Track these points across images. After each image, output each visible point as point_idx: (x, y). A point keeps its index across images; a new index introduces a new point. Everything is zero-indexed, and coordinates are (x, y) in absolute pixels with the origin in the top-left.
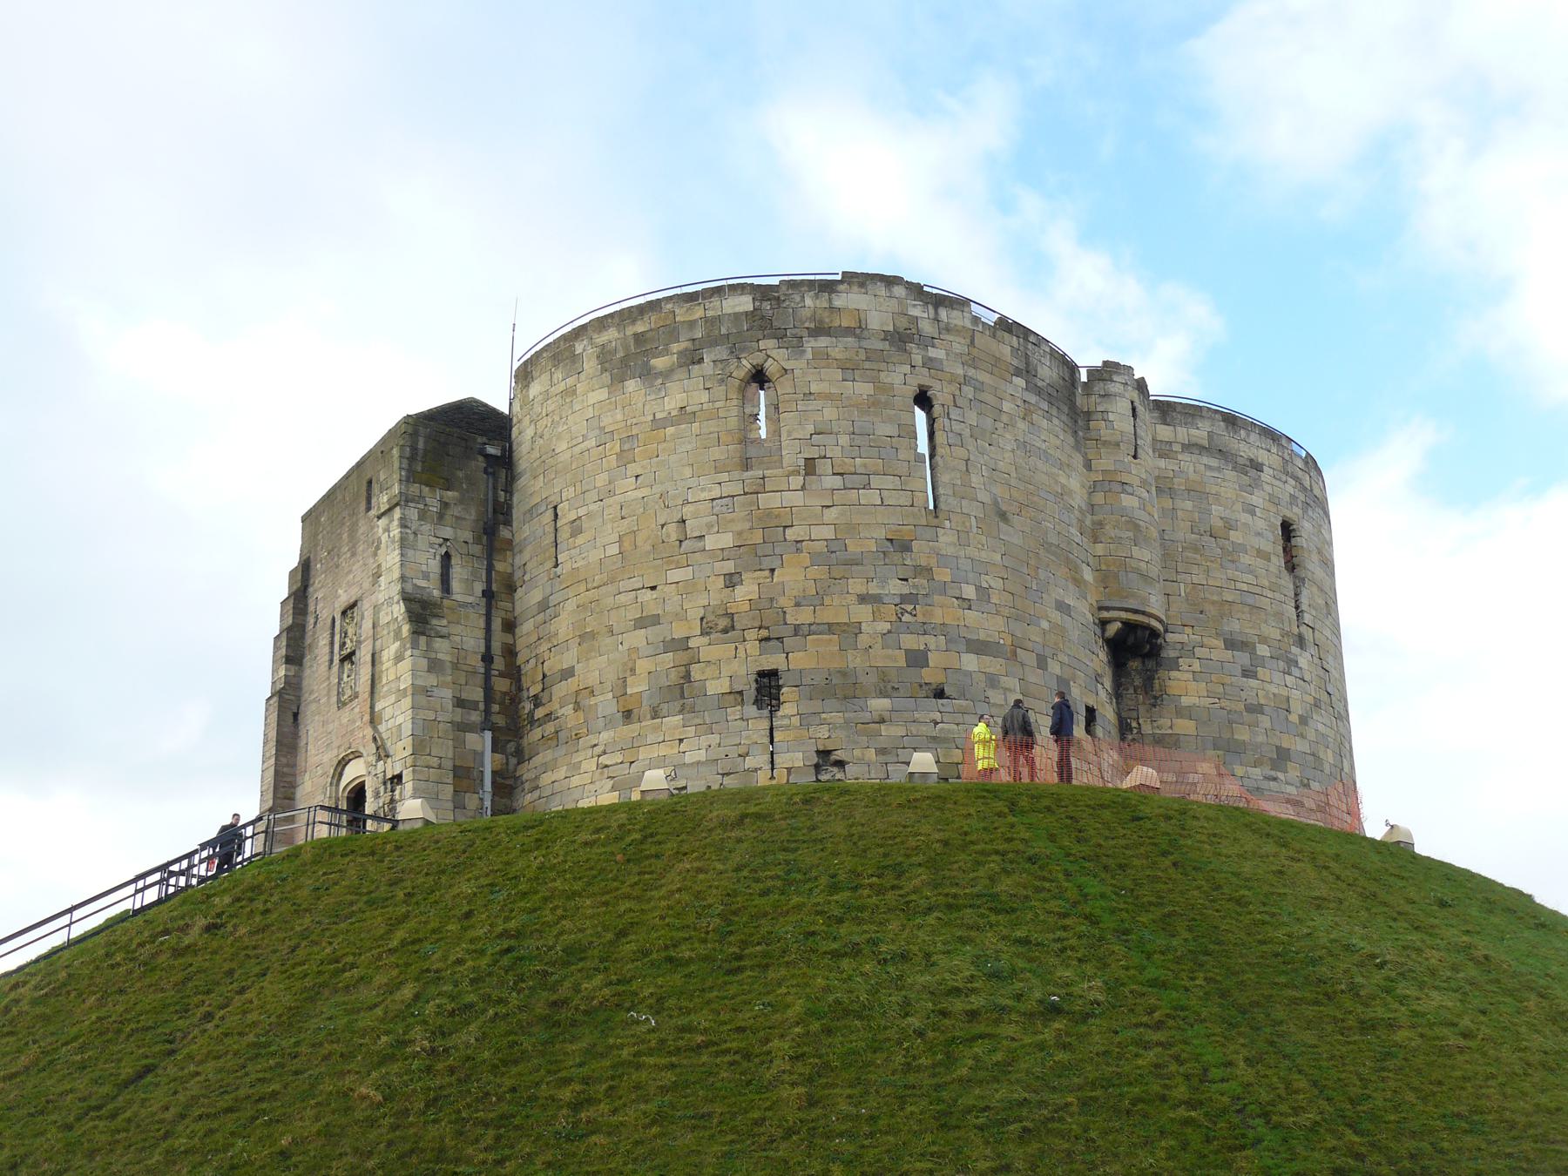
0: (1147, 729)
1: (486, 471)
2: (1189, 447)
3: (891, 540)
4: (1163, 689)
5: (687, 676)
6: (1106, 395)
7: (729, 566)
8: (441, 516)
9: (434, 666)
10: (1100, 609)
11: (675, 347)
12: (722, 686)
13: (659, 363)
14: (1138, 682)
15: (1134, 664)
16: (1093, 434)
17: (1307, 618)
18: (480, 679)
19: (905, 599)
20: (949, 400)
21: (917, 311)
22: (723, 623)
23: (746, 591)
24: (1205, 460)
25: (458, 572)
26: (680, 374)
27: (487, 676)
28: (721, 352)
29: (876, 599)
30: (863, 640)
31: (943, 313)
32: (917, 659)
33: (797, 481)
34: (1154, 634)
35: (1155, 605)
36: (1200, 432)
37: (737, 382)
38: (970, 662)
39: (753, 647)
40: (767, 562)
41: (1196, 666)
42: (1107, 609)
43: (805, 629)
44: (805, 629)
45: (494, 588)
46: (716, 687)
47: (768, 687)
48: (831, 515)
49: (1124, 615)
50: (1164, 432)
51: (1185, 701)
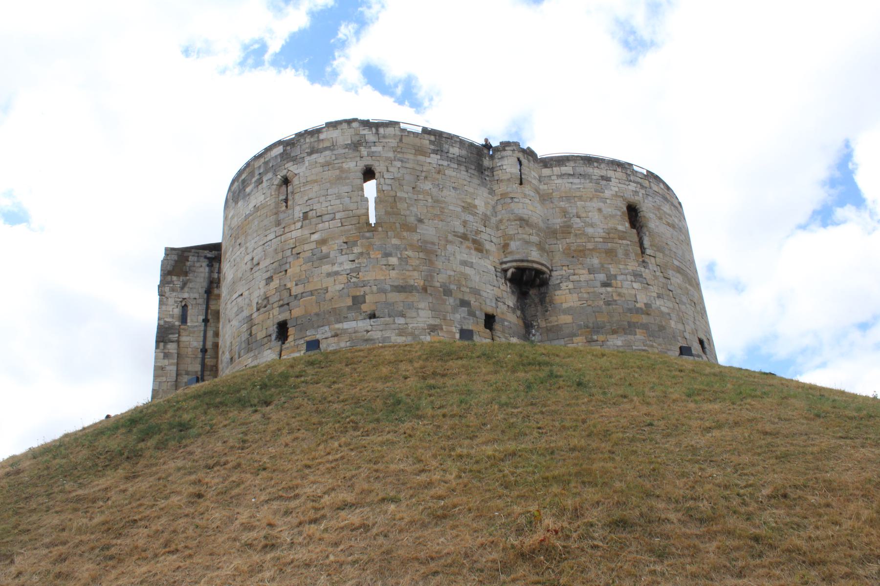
0: (543, 324)
1: (208, 266)
2: (561, 176)
3: (346, 243)
4: (551, 302)
5: (251, 335)
6: (502, 158)
7: (268, 275)
8: (182, 288)
9: (166, 356)
10: (502, 263)
11: (254, 180)
12: (264, 334)
13: (248, 190)
14: (537, 300)
15: (532, 292)
16: (496, 178)
17: (648, 252)
18: (199, 360)
19: (352, 270)
20: (384, 169)
21: (365, 132)
22: (265, 302)
23: (275, 283)
24: (571, 180)
25: (190, 311)
26: (255, 190)
27: (203, 359)
28: (270, 175)
29: (337, 273)
30: (329, 296)
31: (381, 130)
32: (358, 301)
33: (299, 225)
34: (539, 272)
35: (535, 255)
36: (567, 169)
37: (274, 187)
38: (394, 297)
39: (276, 311)
40: (284, 268)
41: (571, 286)
42: (506, 263)
43: (299, 296)
44: (299, 296)
45: (210, 317)
46: (260, 335)
47: (282, 330)
48: (315, 237)
49: (514, 264)
50: (546, 172)
51: (565, 306)
